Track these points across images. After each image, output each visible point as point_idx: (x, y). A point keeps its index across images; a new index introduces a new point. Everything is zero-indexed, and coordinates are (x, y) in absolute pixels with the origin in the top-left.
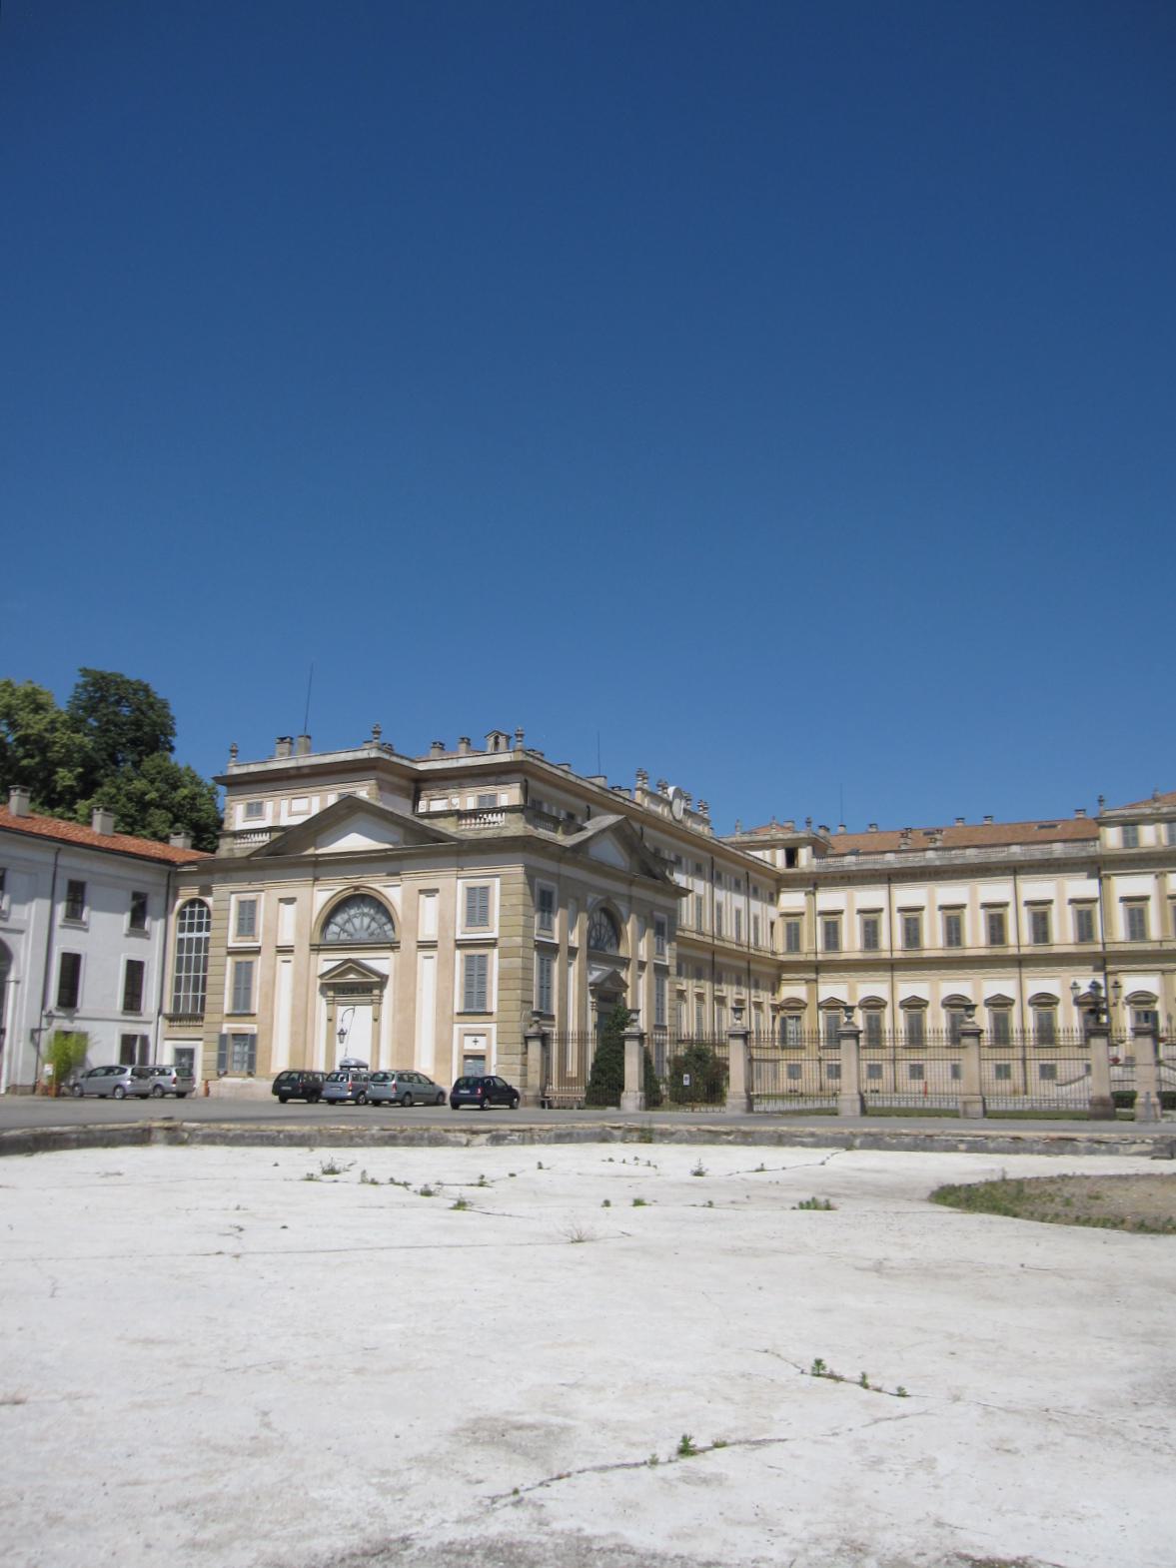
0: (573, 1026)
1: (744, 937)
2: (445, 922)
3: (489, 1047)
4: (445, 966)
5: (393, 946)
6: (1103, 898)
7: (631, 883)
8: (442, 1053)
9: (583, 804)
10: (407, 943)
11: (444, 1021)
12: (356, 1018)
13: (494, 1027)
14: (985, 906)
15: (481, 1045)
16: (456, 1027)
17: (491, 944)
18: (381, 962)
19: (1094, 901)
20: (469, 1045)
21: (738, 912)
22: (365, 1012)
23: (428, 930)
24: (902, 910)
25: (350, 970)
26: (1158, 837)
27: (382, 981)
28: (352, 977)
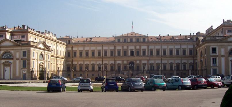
0: (39, 70)
1: (61, 55)
2: (20, 56)
3: (26, 73)
4: (20, 62)
5: (12, 59)
6: (115, 49)
7: (45, 50)
8: (20, 73)
9: (37, 36)
10: (15, 59)
11: (20, 69)
12: (8, 69)
13: (27, 70)
14: (98, 50)
15: (25, 72)
16: (22, 70)
17: (27, 59)
18: (11, 61)
19: (113, 50)
20: (24, 72)
21: (60, 51)
22: (9, 68)
23: (18, 57)
24: (86, 50)
25: (6, 62)
26: (123, 41)
27: (11, 63)
28: (7, 63)
